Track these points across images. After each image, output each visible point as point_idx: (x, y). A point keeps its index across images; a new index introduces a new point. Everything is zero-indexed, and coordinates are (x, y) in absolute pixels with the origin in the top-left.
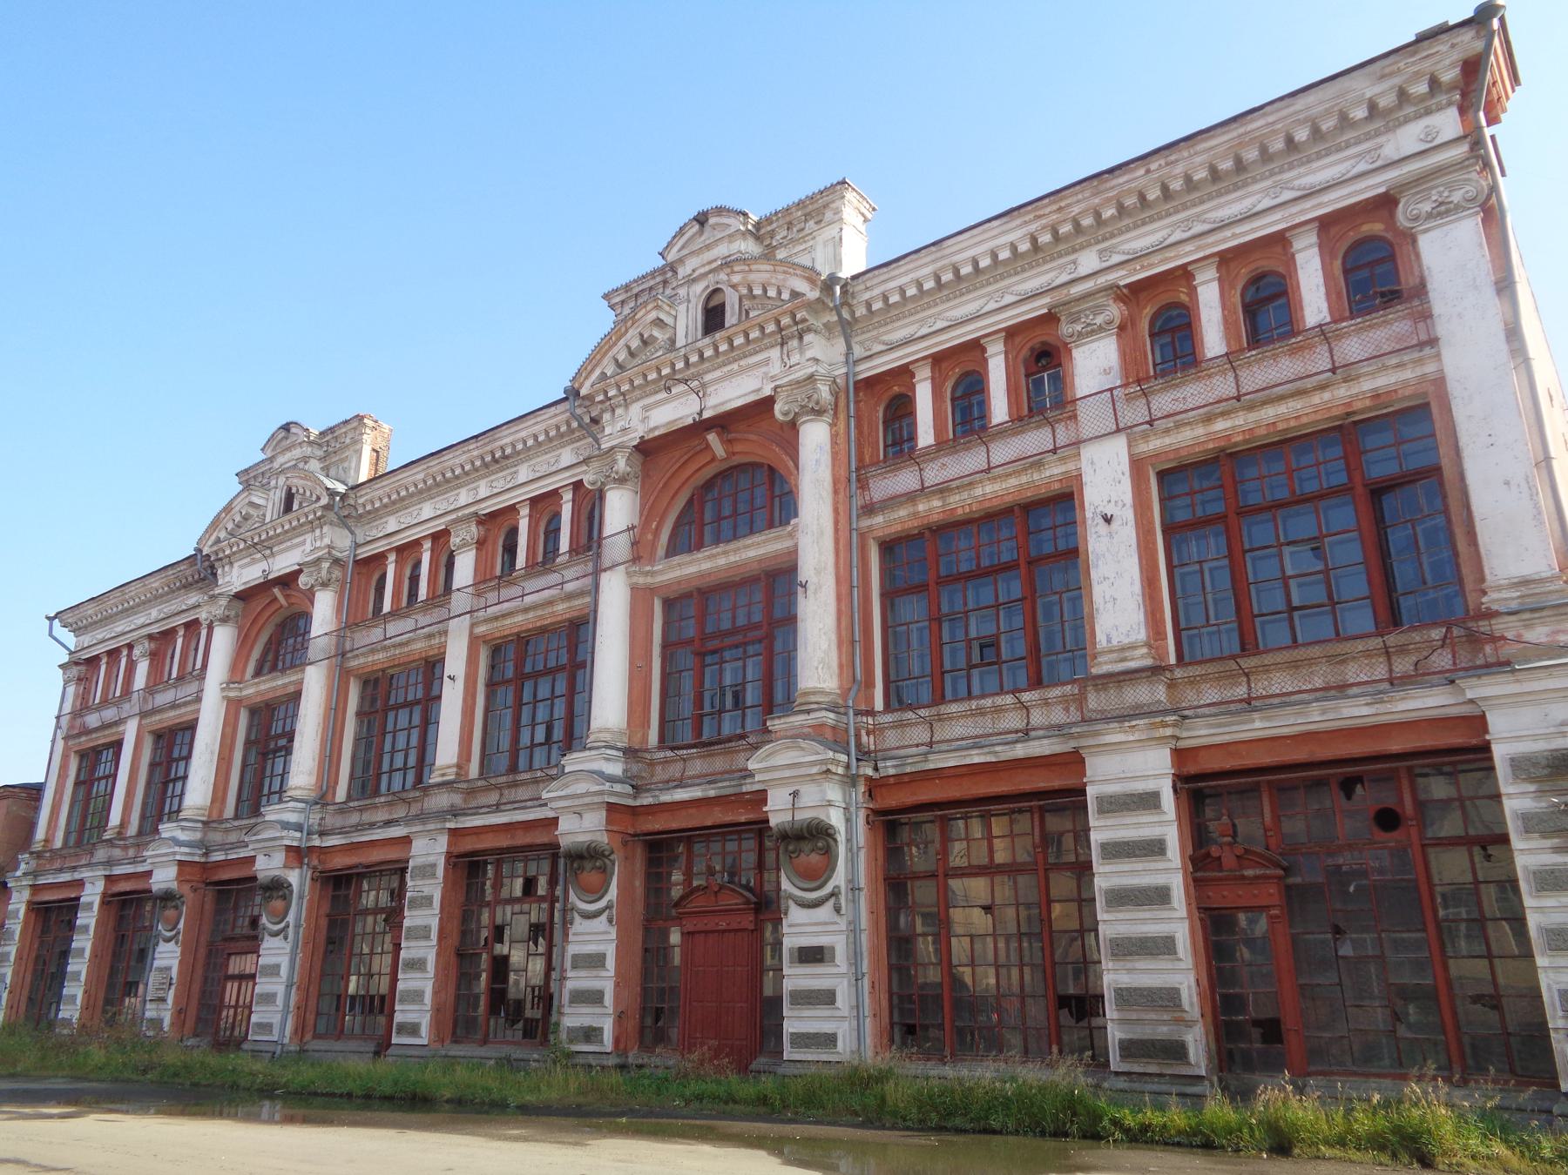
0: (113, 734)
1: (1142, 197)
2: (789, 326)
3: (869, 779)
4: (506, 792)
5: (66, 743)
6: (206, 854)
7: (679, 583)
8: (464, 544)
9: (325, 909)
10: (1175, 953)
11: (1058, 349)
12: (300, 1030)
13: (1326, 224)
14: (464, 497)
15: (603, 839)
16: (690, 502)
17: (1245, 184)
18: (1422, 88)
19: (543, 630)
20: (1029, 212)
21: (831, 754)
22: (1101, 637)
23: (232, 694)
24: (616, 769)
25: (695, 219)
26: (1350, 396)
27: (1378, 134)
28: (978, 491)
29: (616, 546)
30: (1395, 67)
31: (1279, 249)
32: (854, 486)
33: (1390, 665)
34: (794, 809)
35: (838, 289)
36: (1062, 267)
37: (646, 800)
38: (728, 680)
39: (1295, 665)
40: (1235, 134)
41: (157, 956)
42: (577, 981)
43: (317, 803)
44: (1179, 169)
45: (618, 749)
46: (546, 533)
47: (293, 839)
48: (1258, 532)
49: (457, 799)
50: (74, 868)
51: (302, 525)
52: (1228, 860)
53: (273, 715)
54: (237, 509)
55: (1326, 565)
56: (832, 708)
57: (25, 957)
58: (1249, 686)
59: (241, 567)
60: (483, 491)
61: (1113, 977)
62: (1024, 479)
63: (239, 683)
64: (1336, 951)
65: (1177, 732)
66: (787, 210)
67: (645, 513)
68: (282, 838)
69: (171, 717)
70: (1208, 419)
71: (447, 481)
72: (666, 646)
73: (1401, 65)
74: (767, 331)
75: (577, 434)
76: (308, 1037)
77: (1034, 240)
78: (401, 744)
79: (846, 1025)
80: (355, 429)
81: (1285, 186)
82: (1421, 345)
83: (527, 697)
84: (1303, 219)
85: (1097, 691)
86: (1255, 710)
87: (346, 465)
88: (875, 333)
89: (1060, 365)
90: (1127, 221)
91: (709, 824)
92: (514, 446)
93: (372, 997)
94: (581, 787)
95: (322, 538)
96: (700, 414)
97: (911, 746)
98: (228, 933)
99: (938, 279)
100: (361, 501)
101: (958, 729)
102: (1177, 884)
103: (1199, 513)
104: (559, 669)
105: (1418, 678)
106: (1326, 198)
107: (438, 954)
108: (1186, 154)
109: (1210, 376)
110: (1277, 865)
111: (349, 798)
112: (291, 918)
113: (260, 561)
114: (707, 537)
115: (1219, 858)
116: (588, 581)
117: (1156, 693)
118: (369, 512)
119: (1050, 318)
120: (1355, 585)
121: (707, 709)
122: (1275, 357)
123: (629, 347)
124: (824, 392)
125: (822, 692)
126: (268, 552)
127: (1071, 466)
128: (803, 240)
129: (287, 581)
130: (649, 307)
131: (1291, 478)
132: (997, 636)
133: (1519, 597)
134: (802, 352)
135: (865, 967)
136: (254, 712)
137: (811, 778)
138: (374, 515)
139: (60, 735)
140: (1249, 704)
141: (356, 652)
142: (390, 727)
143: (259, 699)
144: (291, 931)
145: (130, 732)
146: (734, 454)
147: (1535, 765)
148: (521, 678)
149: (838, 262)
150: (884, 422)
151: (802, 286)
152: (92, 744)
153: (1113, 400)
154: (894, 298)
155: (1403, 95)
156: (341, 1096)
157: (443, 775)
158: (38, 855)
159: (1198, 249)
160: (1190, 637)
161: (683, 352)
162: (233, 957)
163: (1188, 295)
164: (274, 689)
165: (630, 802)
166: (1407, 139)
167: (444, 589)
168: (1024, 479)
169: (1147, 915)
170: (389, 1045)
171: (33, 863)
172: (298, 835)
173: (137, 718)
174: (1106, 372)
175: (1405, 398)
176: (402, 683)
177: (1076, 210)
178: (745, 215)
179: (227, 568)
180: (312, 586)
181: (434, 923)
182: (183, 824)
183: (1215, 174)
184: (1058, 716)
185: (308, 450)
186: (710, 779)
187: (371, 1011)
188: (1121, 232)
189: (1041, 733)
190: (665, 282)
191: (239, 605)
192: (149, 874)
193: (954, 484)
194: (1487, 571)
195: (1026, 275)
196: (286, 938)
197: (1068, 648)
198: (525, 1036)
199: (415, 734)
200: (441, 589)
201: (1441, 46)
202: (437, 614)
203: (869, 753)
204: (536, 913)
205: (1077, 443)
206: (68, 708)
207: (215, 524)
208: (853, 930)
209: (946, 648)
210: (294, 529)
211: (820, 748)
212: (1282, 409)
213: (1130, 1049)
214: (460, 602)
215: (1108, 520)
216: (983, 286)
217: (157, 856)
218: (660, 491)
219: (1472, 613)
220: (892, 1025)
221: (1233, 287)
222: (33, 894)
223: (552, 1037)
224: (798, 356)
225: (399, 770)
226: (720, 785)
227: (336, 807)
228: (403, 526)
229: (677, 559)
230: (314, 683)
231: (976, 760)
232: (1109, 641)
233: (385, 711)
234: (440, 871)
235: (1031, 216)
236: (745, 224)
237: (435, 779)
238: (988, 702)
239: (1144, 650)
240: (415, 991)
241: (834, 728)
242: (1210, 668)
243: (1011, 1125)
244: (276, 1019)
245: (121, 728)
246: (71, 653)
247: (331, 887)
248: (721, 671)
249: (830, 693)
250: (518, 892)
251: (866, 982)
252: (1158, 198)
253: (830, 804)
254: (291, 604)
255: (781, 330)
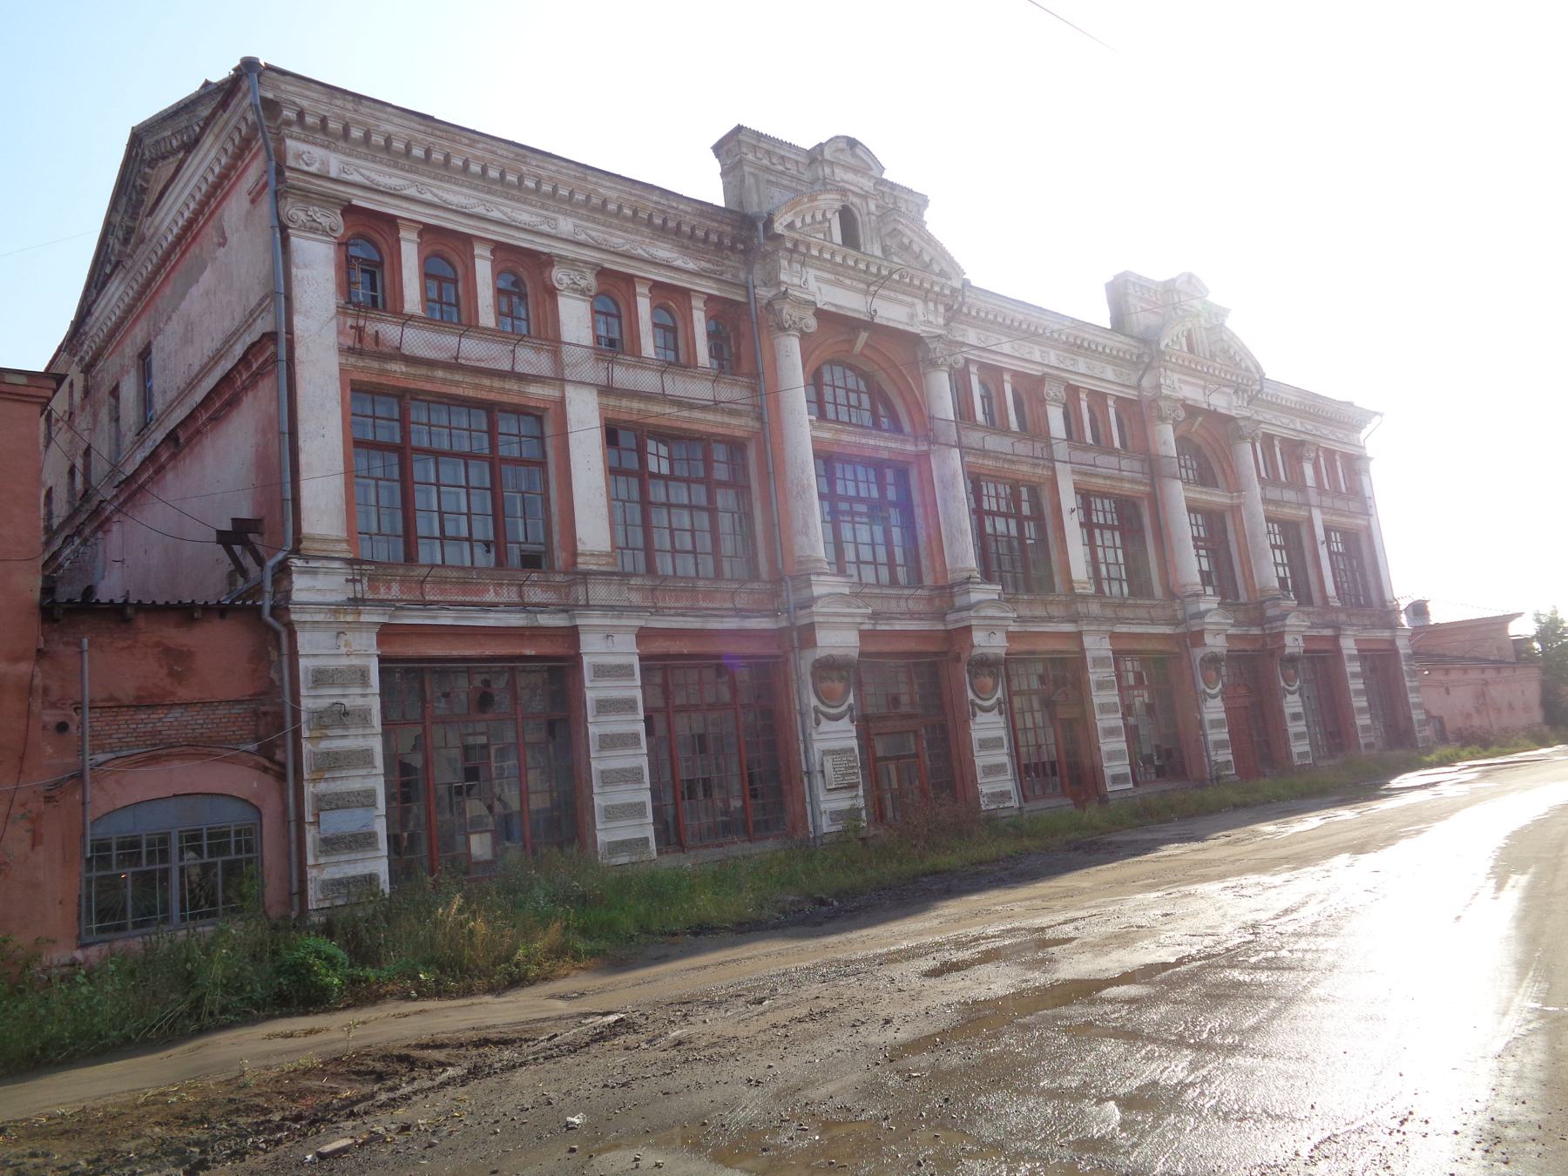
59: (818, 279)
60: (1054, 362)
80: (918, 205)
93: (1044, 763)
164: (862, 446)
196: (1001, 714)
222: (380, 643)
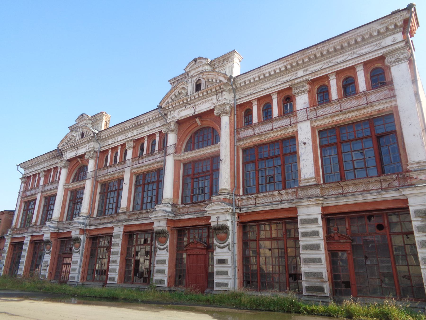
0: (34, 197)
1: (315, 56)
2: (219, 90)
3: (238, 214)
4: (140, 215)
5: (21, 199)
6: (58, 230)
7: (188, 159)
8: (130, 148)
9: (90, 246)
10: (321, 263)
11: (291, 97)
12: (83, 279)
13: (365, 64)
14: (130, 135)
15: (166, 228)
16: (191, 137)
17: (344, 53)
18: (392, 27)
19: (150, 171)
20: (285, 59)
21: (228, 207)
22: (302, 176)
23: (66, 187)
24: (169, 209)
25: (194, 60)
26: (372, 111)
27: (380, 39)
28: (269, 135)
29: (171, 149)
30: (385, 21)
31: (353, 70)
32: (235, 134)
33: (381, 185)
34: (218, 221)
35: (232, 80)
36: (293, 75)
37: (178, 218)
38: (200, 186)
39: (355, 184)
40: (341, 39)
41: (44, 258)
42: (158, 267)
43: (88, 217)
44: (326, 48)
45: (170, 204)
46: (152, 145)
47: (82, 227)
48: (346, 148)
49: (126, 217)
50: (23, 233)
51: (86, 142)
52: (336, 237)
53: (77, 193)
54: (68, 137)
55: (364, 157)
56: (229, 194)
57: (9, 257)
58: (343, 190)
59: (69, 153)
60: (135, 133)
61: (304, 269)
62: (282, 132)
63: (68, 184)
64: (366, 263)
65: (323, 202)
66: (219, 58)
67: (179, 140)
68: (79, 226)
69: (49, 193)
70: (333, 117)
71: (125, 130)
72: (184, 176)
73: (387, 21)
74: (213, 91)
75: (161, 118)
76: (85, 281)
77: (286, 67)
78: (111, 202)
79: (231, 280)
80: (101, 116)
81: (354, 53)
82: (391, 97)
83: (146, 189)
84: (359, 62)
85: (301, 190)
86: (344, 196)
87: (98, 125)
88: (242, 92)
89: (292, 101)
90: (311, 62)
91: (195, 225)
92: (143, 121)
93: (102, 270)
94: (160, 214)
95: (91, 145)
96: (194, 113)
97: (250, 205)
98: (64, 252)
99: (259, 77)
100: (102, 135)
101: (263, 200)
102: (322, 244)
103: (330, 142)
104: (155, 182)
105: (389, 188)
106: (366, 56)
107: (120, 259)
108: (327, 44)
109: (333, 105)
110: (350, 239)
111: (97, 216)
112: (81, 248)
113: (74, 151)
114: (195, 147)
115: (334, 237)
116: (163, 158)
117: (317, 191)
118: (104, 138)
119: (290, 88)
120: (372, 162)
121: (195, 193)
122: (351, 100)
123: (175, 95)
124: (228, 108)
125: (226, 190)
126: (77, 149)
127: (295, 129)
128: (222, 66)
129: (82, 157)
130: (181, 84)
131: (355, 133)
132: (274, 175)
133: (417, 167)
134: (222, 97)
135: (236, 265)
136: (72, 192)
137: (222, 213)
138: (106, 139)
139: (20, 197)
140: (343, 195)
141: (100, 176)
142: (108, 197)
143: (73, 189)
144: (81, 252)
145: (39, 196)
146: (203, 124)
147: (421, 213)
148: (144, 184)
149: (232, 72)
150: (244, 116)
151: (222, 79)
152: (28, 200)
153: (307, 111)
154: (247, 83)
155: (387, 29)
156: (93, 297)
157: (123, 210)
158: (13, 230)
159: (331, 70)
160: (326, 176)
161: (190, 96)
162: (65, 259)
163: (328, 83)
164: (78, 186)
165: (173, 219)
166: (388, 41)
167: (163, 147)
168: (282, 132)
169: (314, 252)
170: (107, 283)
171: (12, 232)
172: (83, 226)
173: (41, 193)
174: (305, 103)
175: (387, 112)
176: (112, 185)
177: (297, 59)
178: (207, 59)
179: (65, 153)
180: (88, 158)
181: (120, 251)
182: (52, 222)
183: (335, 50)
184: (290, 197)
185: (88, 121)
186: (195, 213)
187: (102, 274)
188: (309, 65)
189: (285, 202)
190: (185, 77)
191: (68, 163)
192: (43, 235)
193: (263, 134)
194: (408, 159)
195: (283, 77)
196: (79, 254)
197: (293, 179)
198: (143, 282)
199: (115, 199)
200: (123, 160)
201: (398, 16)
202: (122, 166)
203: (238, 206)
204: (147, 248)
205: (297, 123)
206: (22, 190)
207: (62, 141)
208: (233, 255)
209: (260, 178)
210: (84, 142)
211: (225, 205)
212: (353, 114)
213: (309, 289)
214: (128, 163)
215: (305, 144)
216: (272, 80)
217: (45, 230)
218: (183, 134)
219: (404, 171)
220: (243, 281)
221: (340, 81)
222: (11, 240)
223: (151, 282)
224: (221, 98)
225: (111, 208)
226: (198, 214)
227: (93, 218)
228: (113, 142)
229: (187, 153)
230: (88, 184)
231: (268, 209)
232: (304, 177)
233: (108, 192)
234: (121, 236)
235: (285, 61)
236: (207, 62)
237: (120, 211)
238: (271, 193)
239: (314, 180)
240: (114, 269)
241: (229, 199)
242: (332, 185)
243: (275, 309)
244: (76, 276)
245: (36, 196)
246: (23, 175)
247: (92, 240)
248: (199, 183)
249: (228, 190)
250: (142, 242)
251: (237, 269)
252: (320, 56)
253: (227, 220)
254: (82, 163)
255: (216, 91)
